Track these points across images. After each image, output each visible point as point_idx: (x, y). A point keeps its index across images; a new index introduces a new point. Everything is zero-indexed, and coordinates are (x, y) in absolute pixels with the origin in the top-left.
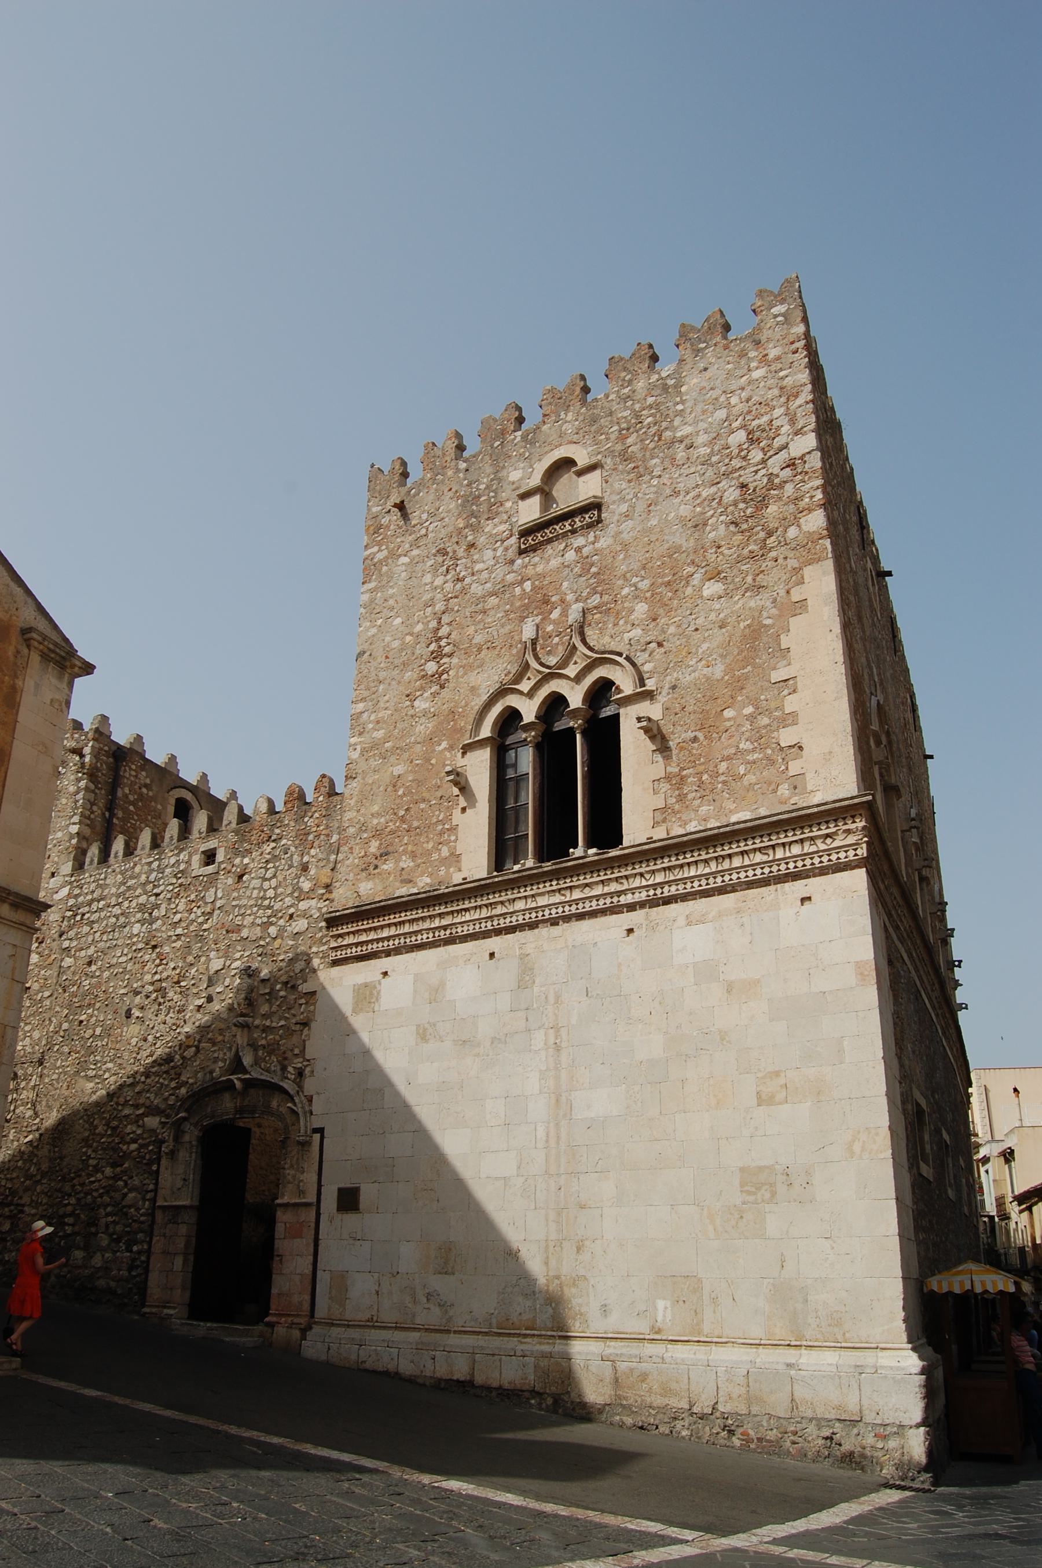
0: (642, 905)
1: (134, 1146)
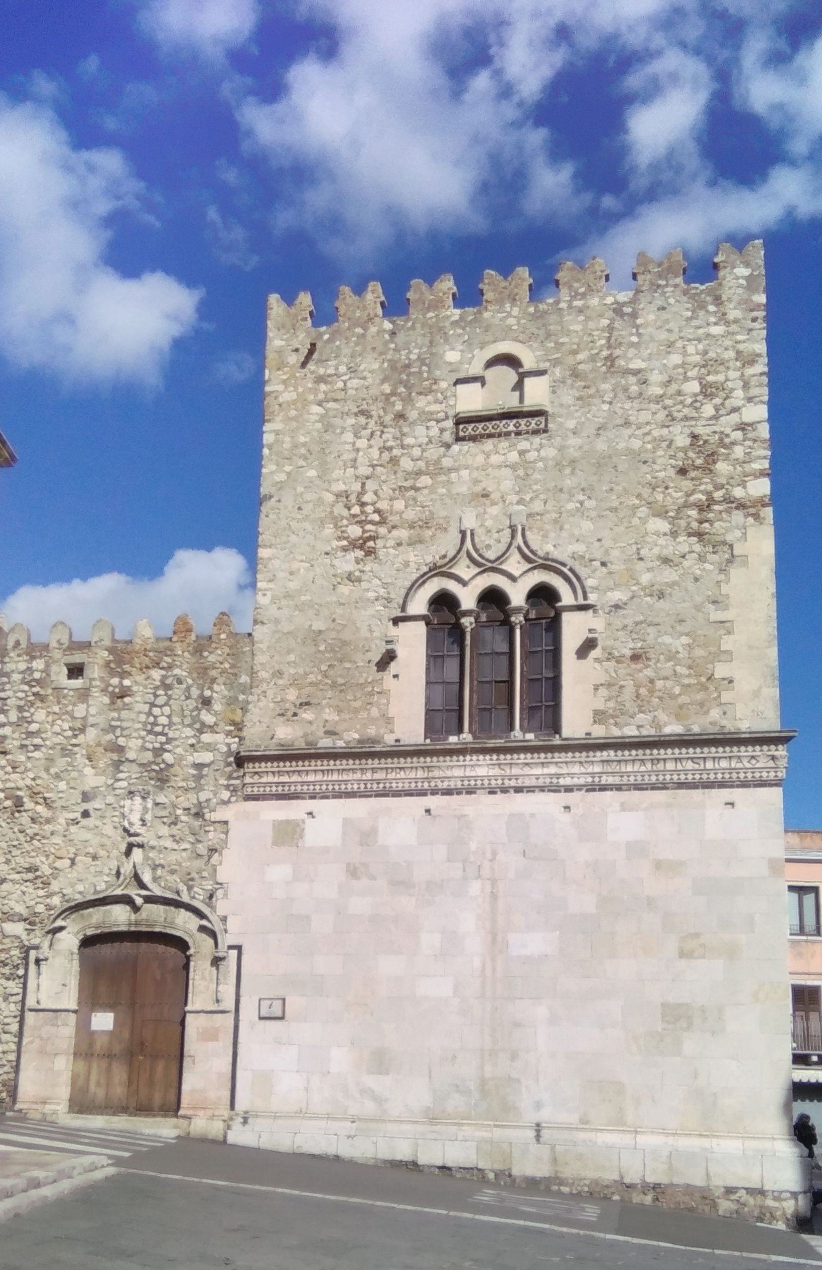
0: (579, 788)
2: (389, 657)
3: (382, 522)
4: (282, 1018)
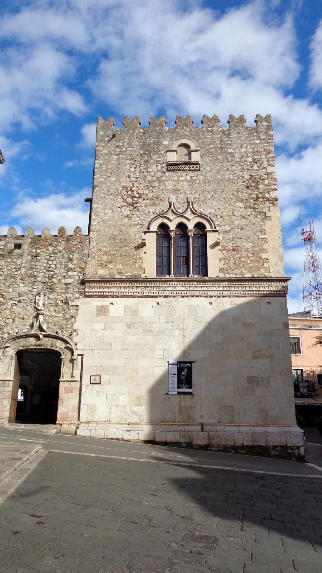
2: (143, 245)
3: (140, 197)
4: (100, 383)
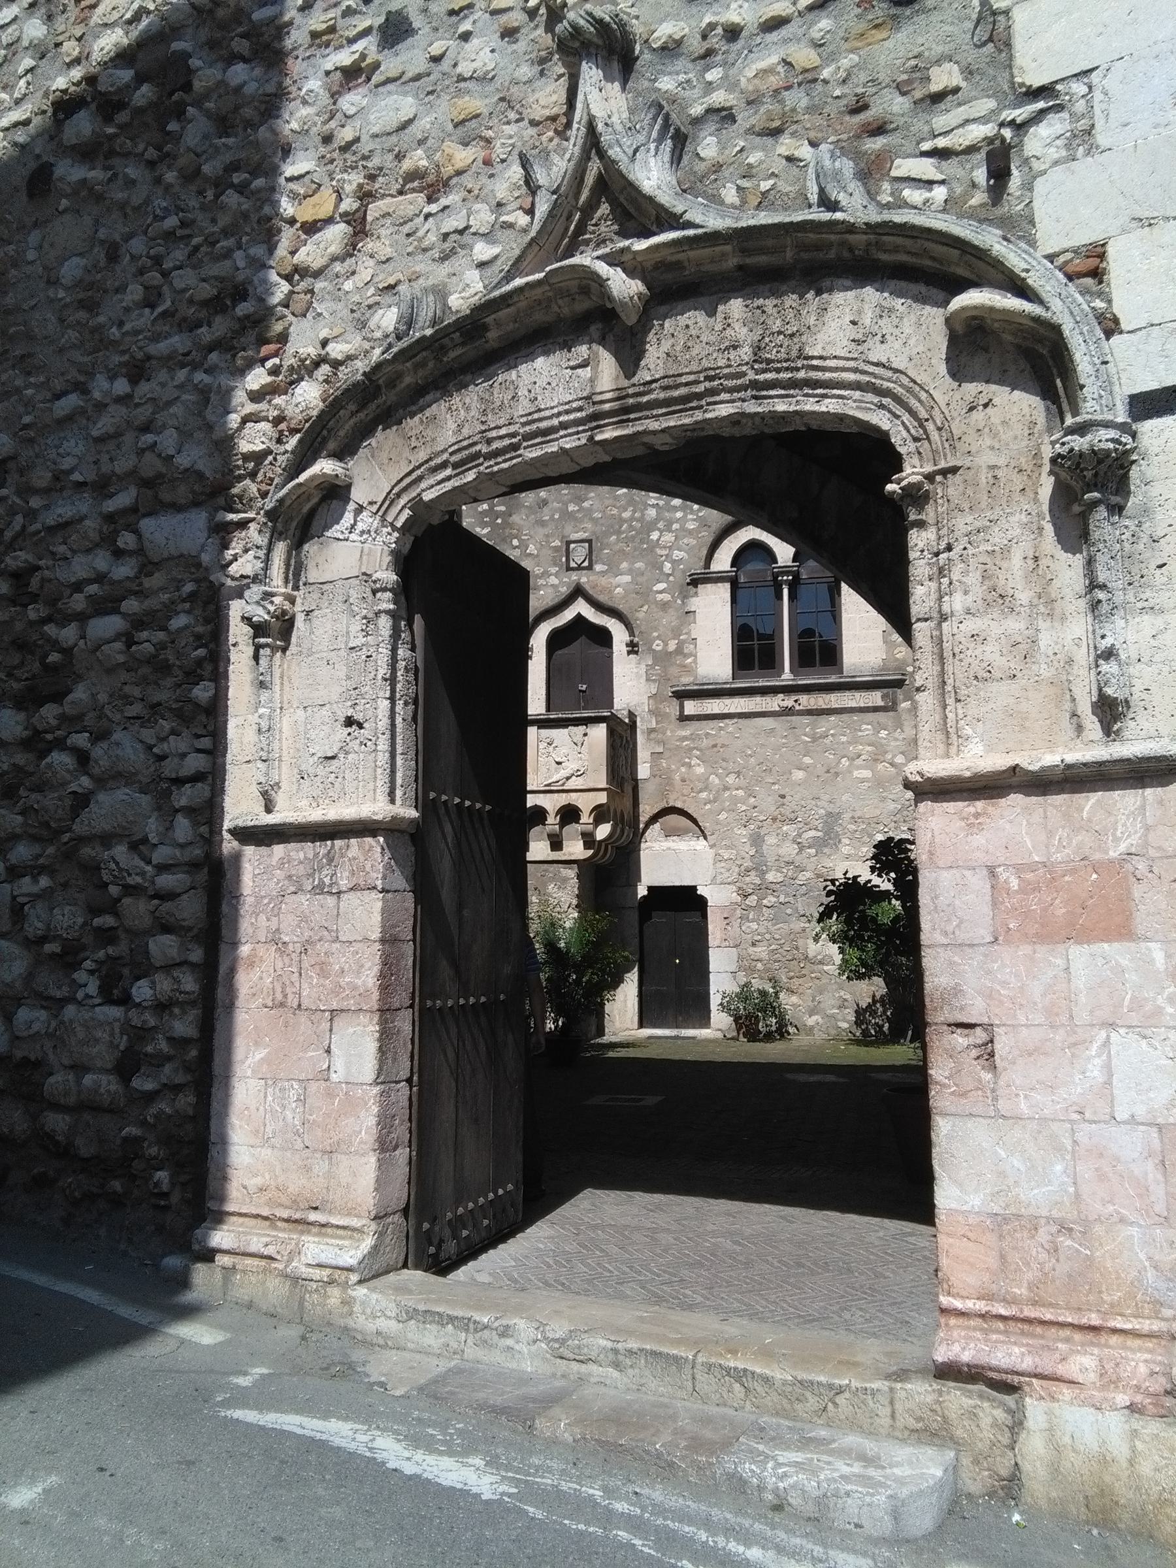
1: (107, 626)
